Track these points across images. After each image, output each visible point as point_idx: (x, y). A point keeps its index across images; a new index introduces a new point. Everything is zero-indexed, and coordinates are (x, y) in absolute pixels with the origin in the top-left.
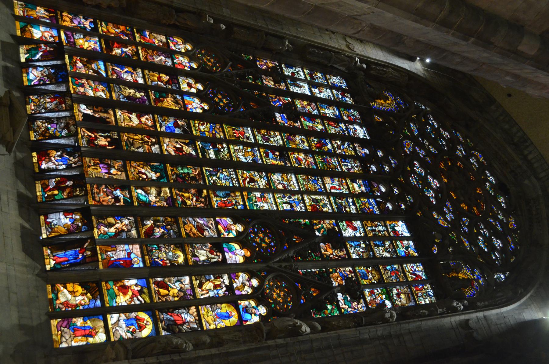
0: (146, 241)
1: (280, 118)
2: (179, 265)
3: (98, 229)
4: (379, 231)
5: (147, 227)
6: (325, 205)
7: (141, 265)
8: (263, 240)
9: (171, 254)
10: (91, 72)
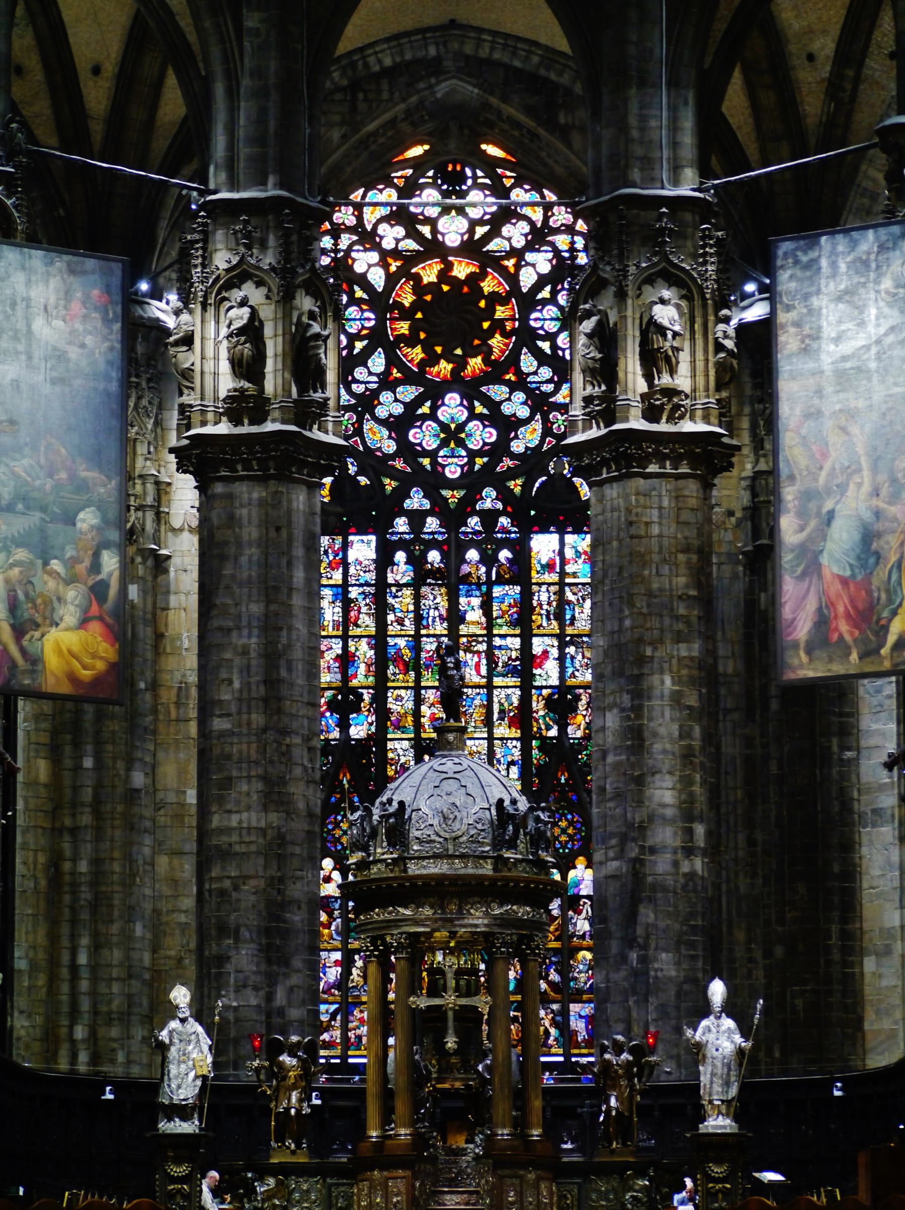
0: (567, 993)
1: (359, 728)
2: (594, 959)
3: (551, 1046)
4: (549, 604)
5: (549, 990)
6: (508, 696)
7: (592, 1005)
8: (564, 831)
9: (581, 967)
10: (337, 1023)
